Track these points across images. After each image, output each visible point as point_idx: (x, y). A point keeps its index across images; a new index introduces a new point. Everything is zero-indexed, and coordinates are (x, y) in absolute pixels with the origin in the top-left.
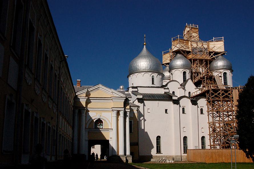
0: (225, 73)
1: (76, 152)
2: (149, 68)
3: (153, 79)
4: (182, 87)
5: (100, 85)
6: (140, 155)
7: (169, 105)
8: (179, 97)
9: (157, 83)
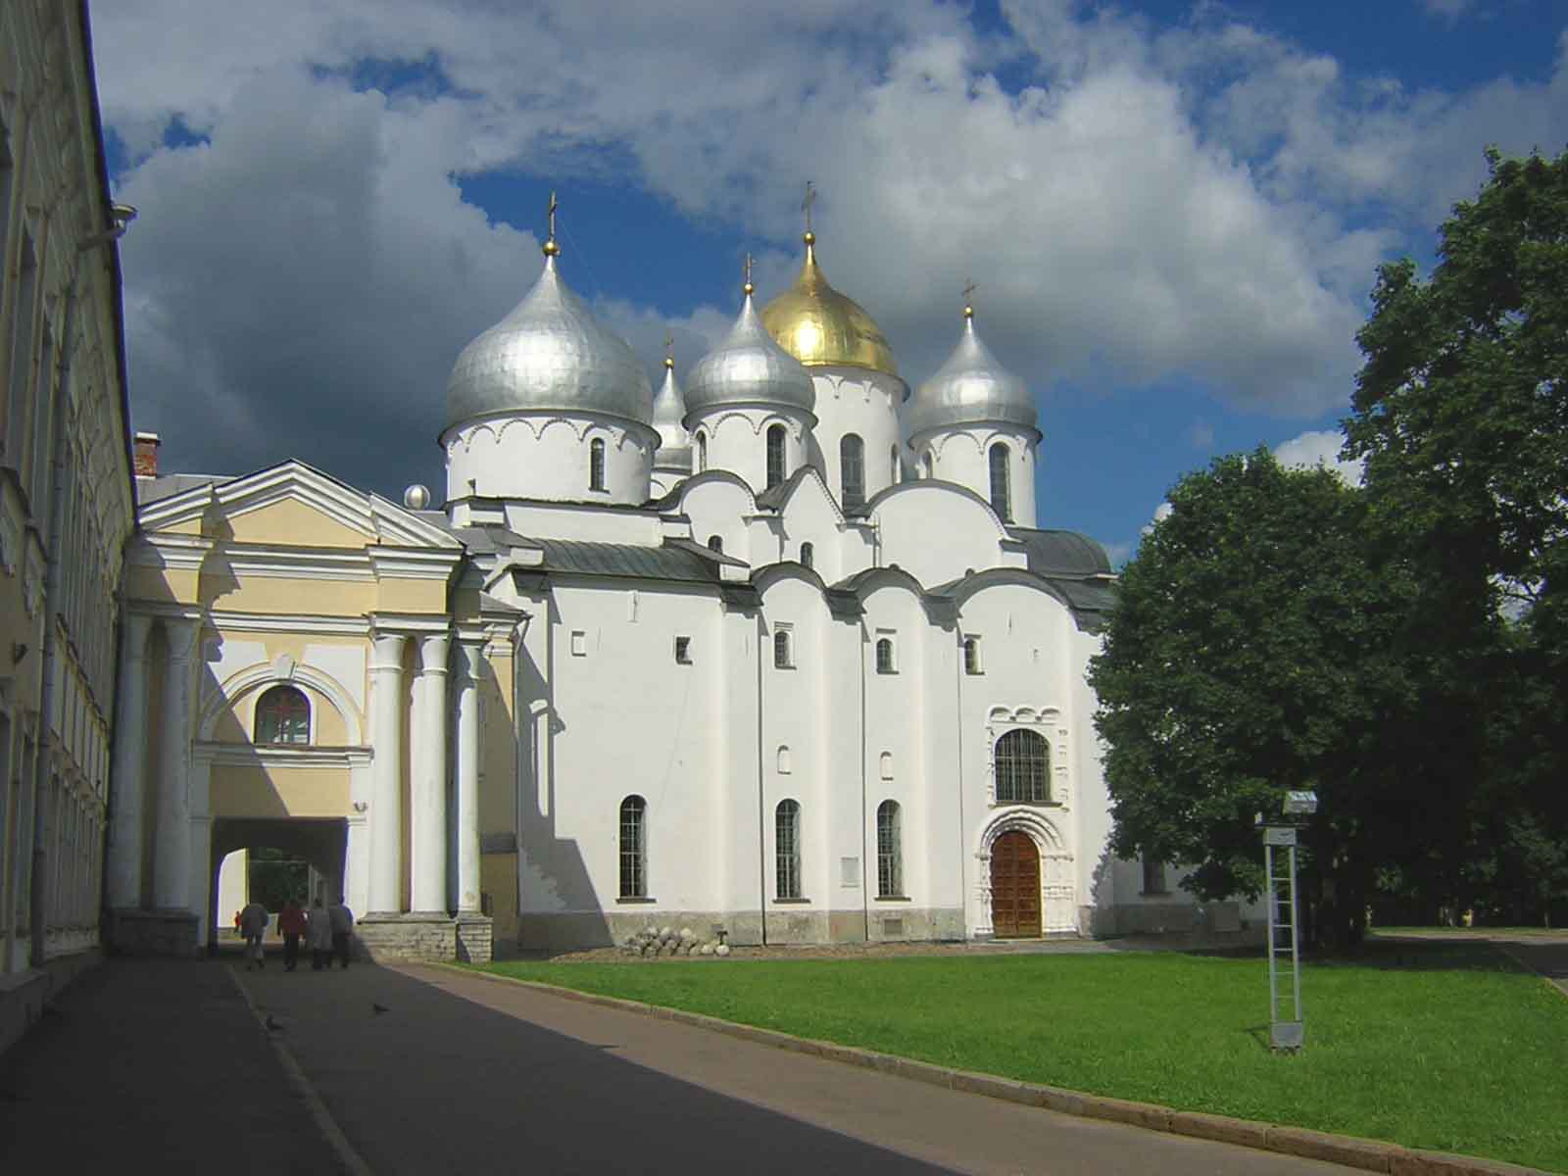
0: (999, 453)
2: (574, 391)
3: (596, 458)
4: (768, 513)
5: (298, 470)
6: (523, 910)
8: (754, 568)
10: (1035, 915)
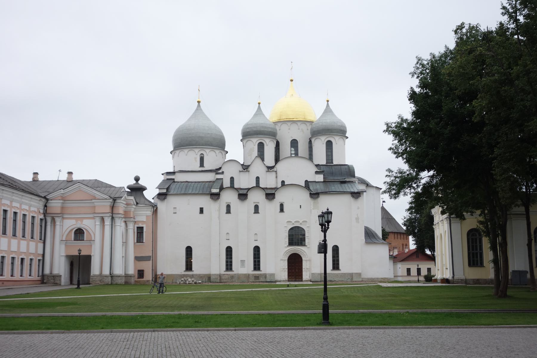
1: (47, 271)
3: (202, 159)
7: (204, 201)
9: (207, 166)
10: (301, 275)
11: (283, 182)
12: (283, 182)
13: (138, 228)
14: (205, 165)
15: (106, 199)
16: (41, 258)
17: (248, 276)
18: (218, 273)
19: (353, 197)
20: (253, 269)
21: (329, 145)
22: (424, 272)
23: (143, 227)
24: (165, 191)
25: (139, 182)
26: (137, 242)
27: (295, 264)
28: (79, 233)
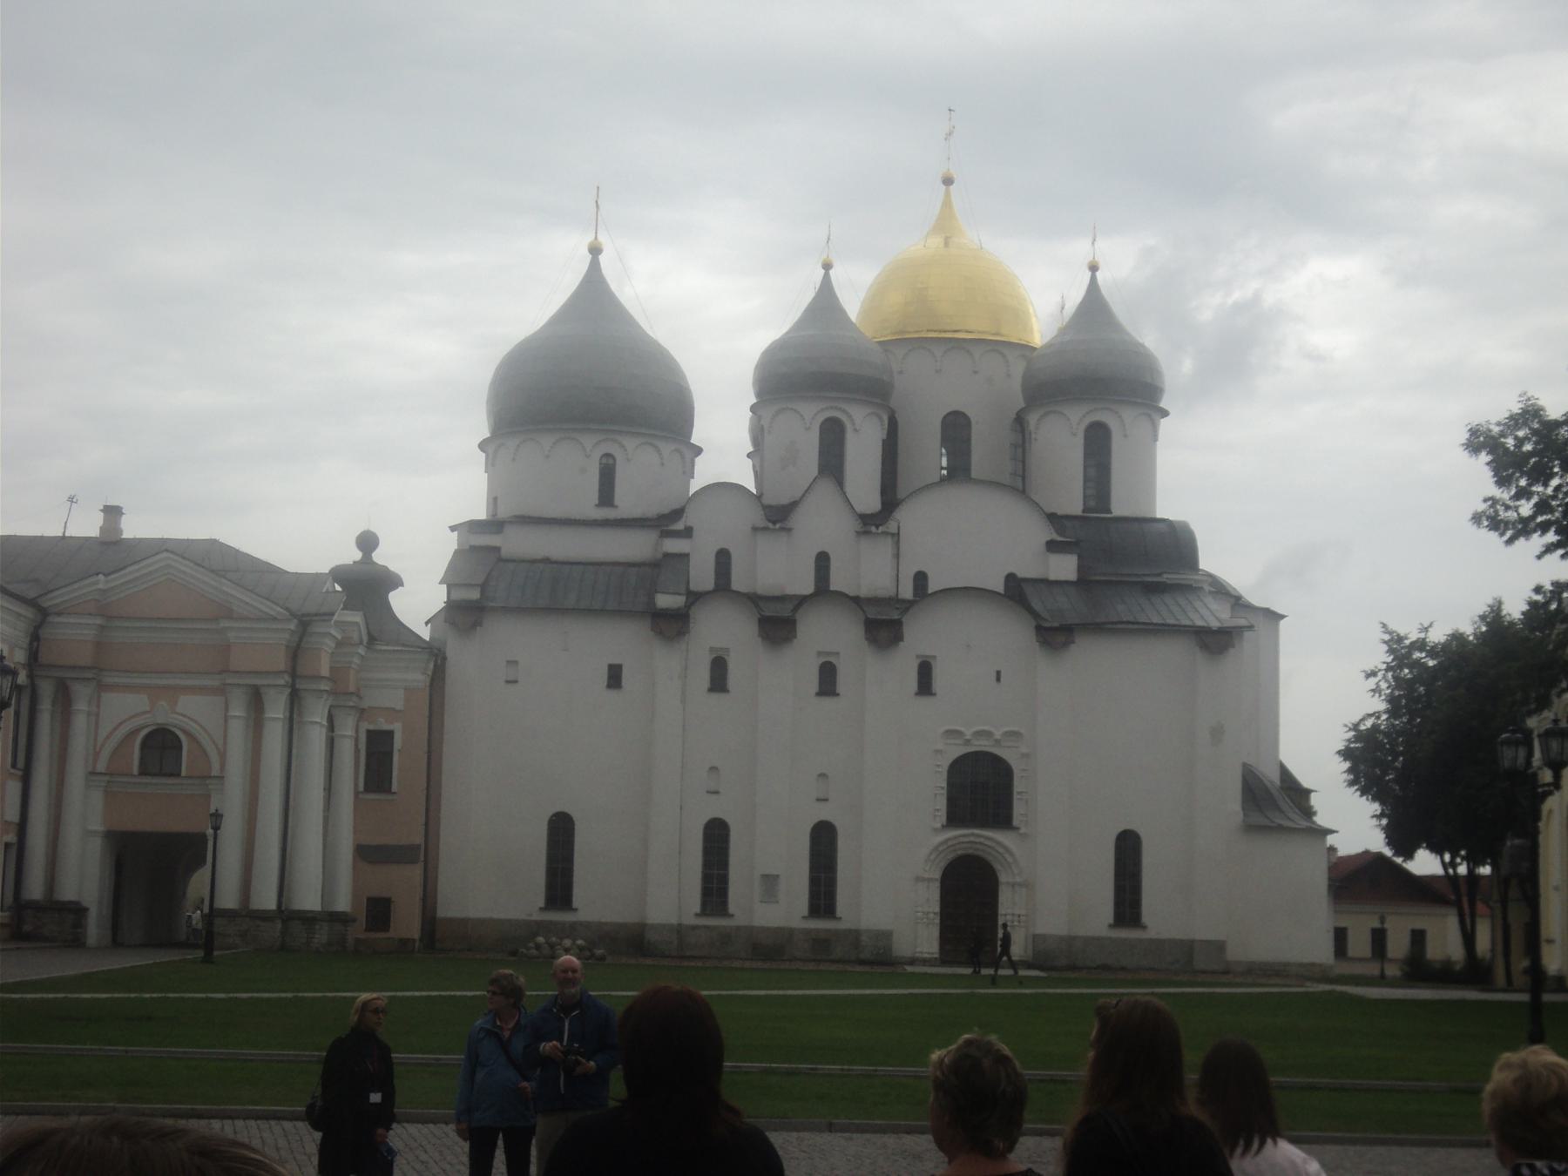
1: (35, 889)
11: (921, 579)
12: (921, 579)
13: (369, 732)
14: (617, 501)
15: (275, 619)
16: (11, 837)
17: (787, 934)
18: (674, 921)
19: (1205, 647)
20: (805, 912)
21: (1098, 442)
22: (1398, 946)
23: (390, 734)
24: (474, 595)
25: (379, 557)
26: (367, 789)
27: (969, 892)
28: (161, 749)
